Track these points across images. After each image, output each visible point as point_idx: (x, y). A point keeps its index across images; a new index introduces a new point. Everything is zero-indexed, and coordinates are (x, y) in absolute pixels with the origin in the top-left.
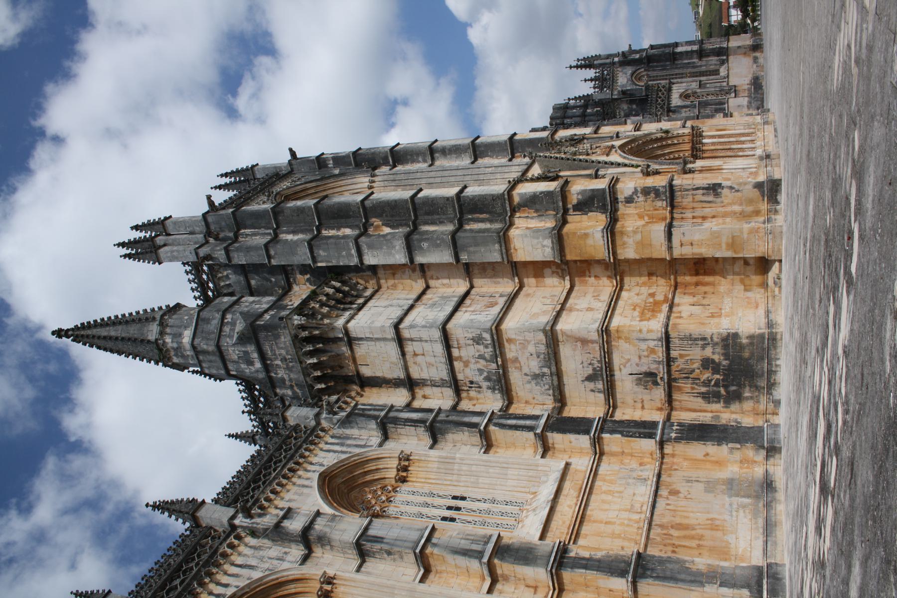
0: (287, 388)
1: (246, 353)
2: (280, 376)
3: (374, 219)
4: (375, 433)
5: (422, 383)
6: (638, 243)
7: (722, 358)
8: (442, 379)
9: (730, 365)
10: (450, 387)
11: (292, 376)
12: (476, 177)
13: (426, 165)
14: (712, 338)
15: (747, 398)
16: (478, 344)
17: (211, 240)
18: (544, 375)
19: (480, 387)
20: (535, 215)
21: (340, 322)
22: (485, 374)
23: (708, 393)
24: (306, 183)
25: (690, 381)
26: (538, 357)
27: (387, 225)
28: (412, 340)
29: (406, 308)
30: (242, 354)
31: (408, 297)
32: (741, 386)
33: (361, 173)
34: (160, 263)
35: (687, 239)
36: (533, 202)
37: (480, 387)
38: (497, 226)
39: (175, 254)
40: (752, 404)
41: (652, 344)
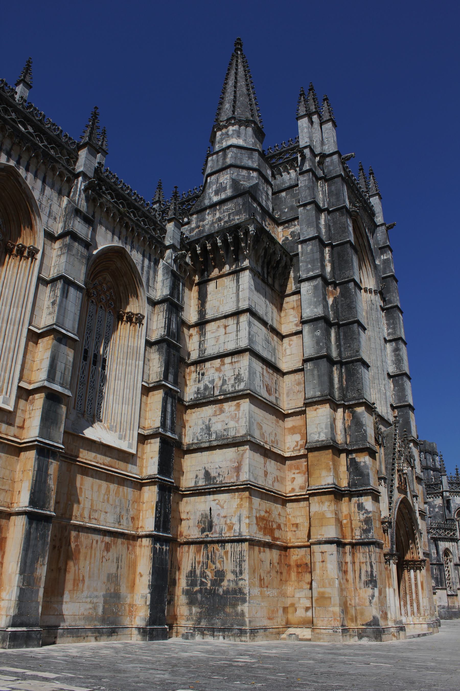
1: (225, 189)
2: (207, 217)
5: (202, 333)
6: (323, 514)
7: (225, 588)
8: (205, 350)
9: (218, 595)
10: (199, 357)
11: (207, 227)
14: (242, 579)
15: (190, 610)
16: (235, 379)
17: (318, 159)
18: (210, 435)
19: (199, 382)
20: (346, 426)
22: (210, 386)
23: (195, 575)
25: (205, 560)
26: (225, 430)
28: (238, 323)
29: (265, 318)
30: (224, 185)
31: (275, 321)
32: (201, 605)
37: (199, 382)
40: (185, 614)
41: (236, 527)
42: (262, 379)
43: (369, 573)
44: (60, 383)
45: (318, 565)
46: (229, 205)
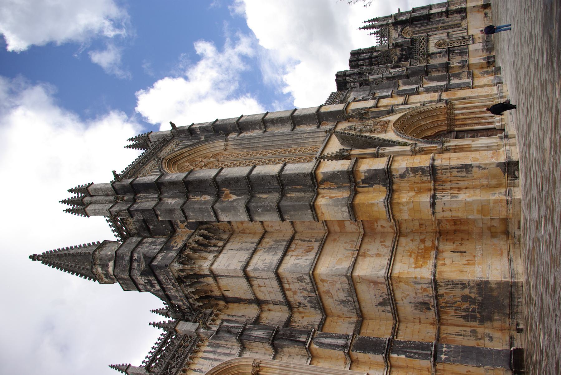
0: (179, 301)
1: (149, 280)
2: (173, 294)
3: (224, 189)
4: (236, 344)
5: (267, 302)
6: (410, 210)
7: (477, 296)
8: (279, 301)
9: (482, 300)
12: (295, 141)
13: (262, 131)
14: (468, 283)
15: (497, 320)
18: (349, 301)
19: (306, 306)
20: (335, 186)
21: (206, 264)
22: (308, 299)
23: (467, 316)
24: (182, 149)
25: (454, 308)
26: (344, 291)
28: (256, 278)
34: (88, 217)
35: (447, 207)
38: (309, 195)
39: (97, 211)
40: (500, 323)
41: (424, 286)
42: (300, 257)
43: (459, 170)
45: (454, 214)
46: (162, 278)
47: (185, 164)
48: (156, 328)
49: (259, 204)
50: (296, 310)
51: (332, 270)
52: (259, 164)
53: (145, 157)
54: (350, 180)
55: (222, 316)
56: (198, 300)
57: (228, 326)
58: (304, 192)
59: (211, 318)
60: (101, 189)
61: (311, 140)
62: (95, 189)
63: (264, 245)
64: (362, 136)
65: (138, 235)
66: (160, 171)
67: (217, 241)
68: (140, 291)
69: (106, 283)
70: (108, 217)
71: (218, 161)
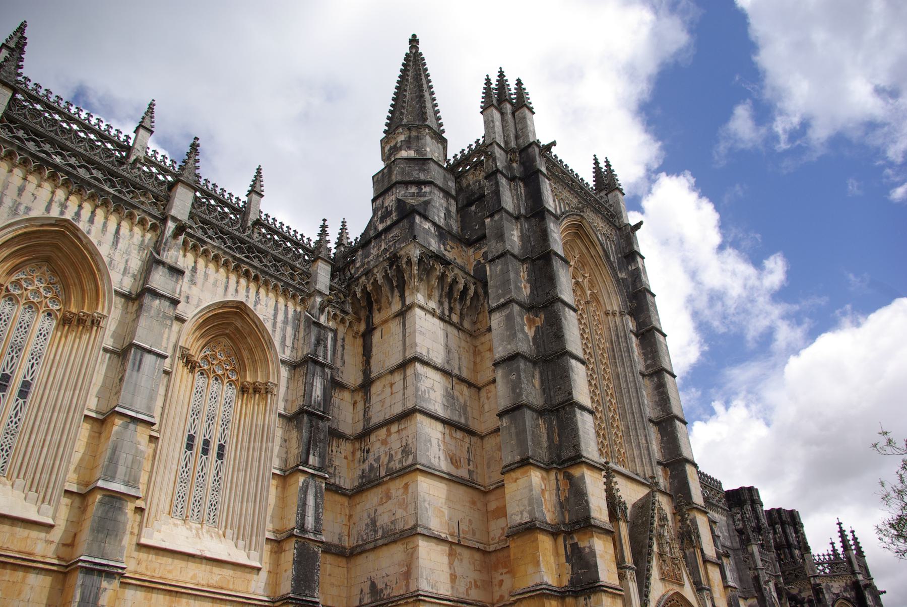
1: (390, 213)
3: (543, 316)
4: (300, 354)
5: (367, 399)
8: (370, 418)
13: (643, 369)
18: (376, 531)
20: (562, 499)
21: (420, 298)
22: (376, 465)
24: (601, 245)
26: (392, 523)
27: (537, 332)
28: (405, 378)
30: (389, 209)
33: (624, 302)
34: (481, 113)
36: (576, 495)
39: (491, 125)
42: (442, 447)
44: (124, 481)
46: (395, 232)
47: (577, 252)
48: (319, 230)
49: (523, 375)
50: (357, 445)
51: (425, 501)
52: (588, 368)
53: (582, 188)
54: (574, 524)
55: (341, 330)
56: (364, 289)
57: (327, 339)
58: (549, 447)
59: (338, 312)
60: (525, 126)
61: (636, 452)
62: (524, 118)
63: (457, 387)
64: (651, 539)
65: (459, 190)
66: (563, 213)
67: (458, 312)
68: (374, 201)
69: (383, 148)
70: (484, 141)
71: (587, 303)
